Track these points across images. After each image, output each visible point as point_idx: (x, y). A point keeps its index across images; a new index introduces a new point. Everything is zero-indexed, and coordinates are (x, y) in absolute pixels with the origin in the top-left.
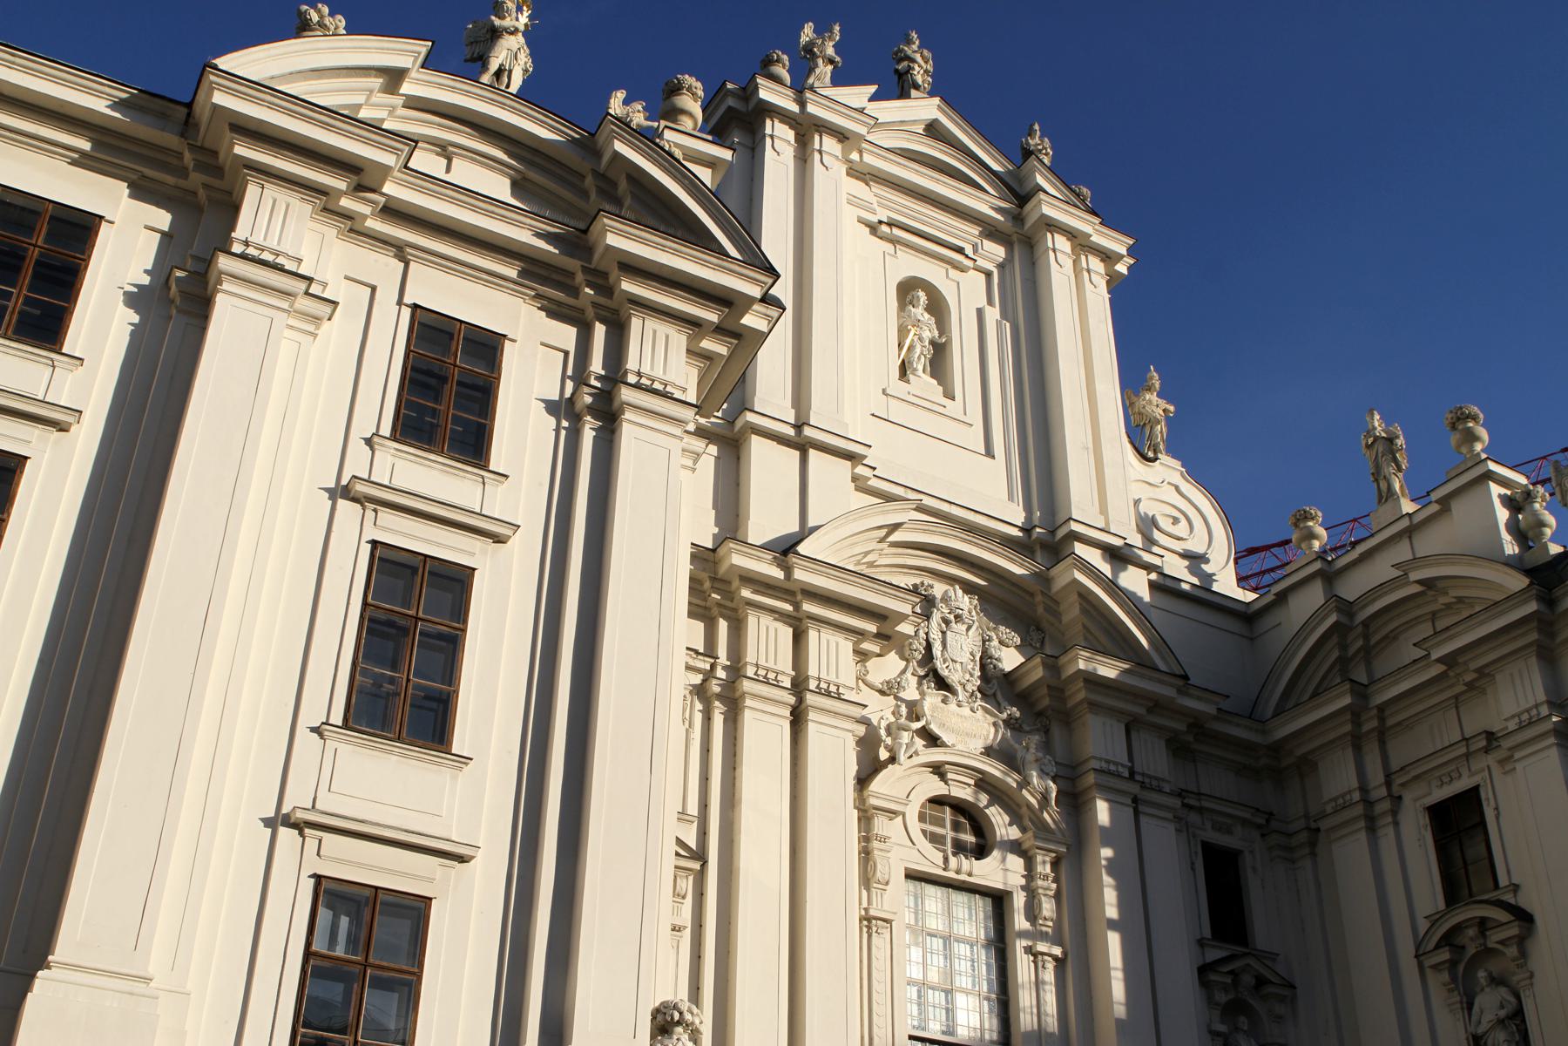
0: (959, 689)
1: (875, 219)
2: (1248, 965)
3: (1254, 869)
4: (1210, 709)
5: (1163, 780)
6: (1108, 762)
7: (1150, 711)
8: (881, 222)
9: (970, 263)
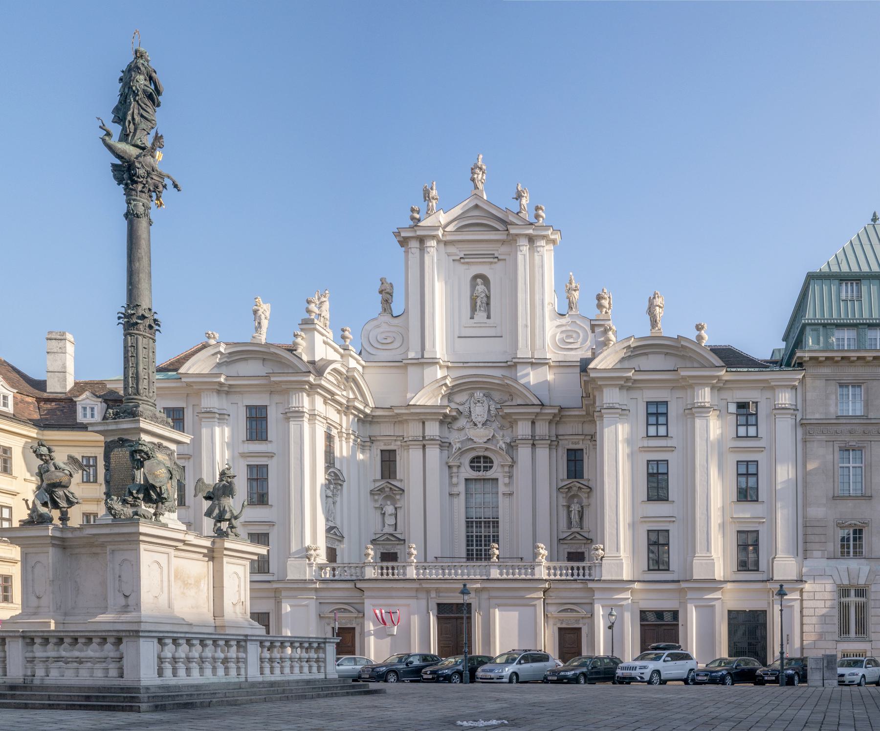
3: (586, 453)
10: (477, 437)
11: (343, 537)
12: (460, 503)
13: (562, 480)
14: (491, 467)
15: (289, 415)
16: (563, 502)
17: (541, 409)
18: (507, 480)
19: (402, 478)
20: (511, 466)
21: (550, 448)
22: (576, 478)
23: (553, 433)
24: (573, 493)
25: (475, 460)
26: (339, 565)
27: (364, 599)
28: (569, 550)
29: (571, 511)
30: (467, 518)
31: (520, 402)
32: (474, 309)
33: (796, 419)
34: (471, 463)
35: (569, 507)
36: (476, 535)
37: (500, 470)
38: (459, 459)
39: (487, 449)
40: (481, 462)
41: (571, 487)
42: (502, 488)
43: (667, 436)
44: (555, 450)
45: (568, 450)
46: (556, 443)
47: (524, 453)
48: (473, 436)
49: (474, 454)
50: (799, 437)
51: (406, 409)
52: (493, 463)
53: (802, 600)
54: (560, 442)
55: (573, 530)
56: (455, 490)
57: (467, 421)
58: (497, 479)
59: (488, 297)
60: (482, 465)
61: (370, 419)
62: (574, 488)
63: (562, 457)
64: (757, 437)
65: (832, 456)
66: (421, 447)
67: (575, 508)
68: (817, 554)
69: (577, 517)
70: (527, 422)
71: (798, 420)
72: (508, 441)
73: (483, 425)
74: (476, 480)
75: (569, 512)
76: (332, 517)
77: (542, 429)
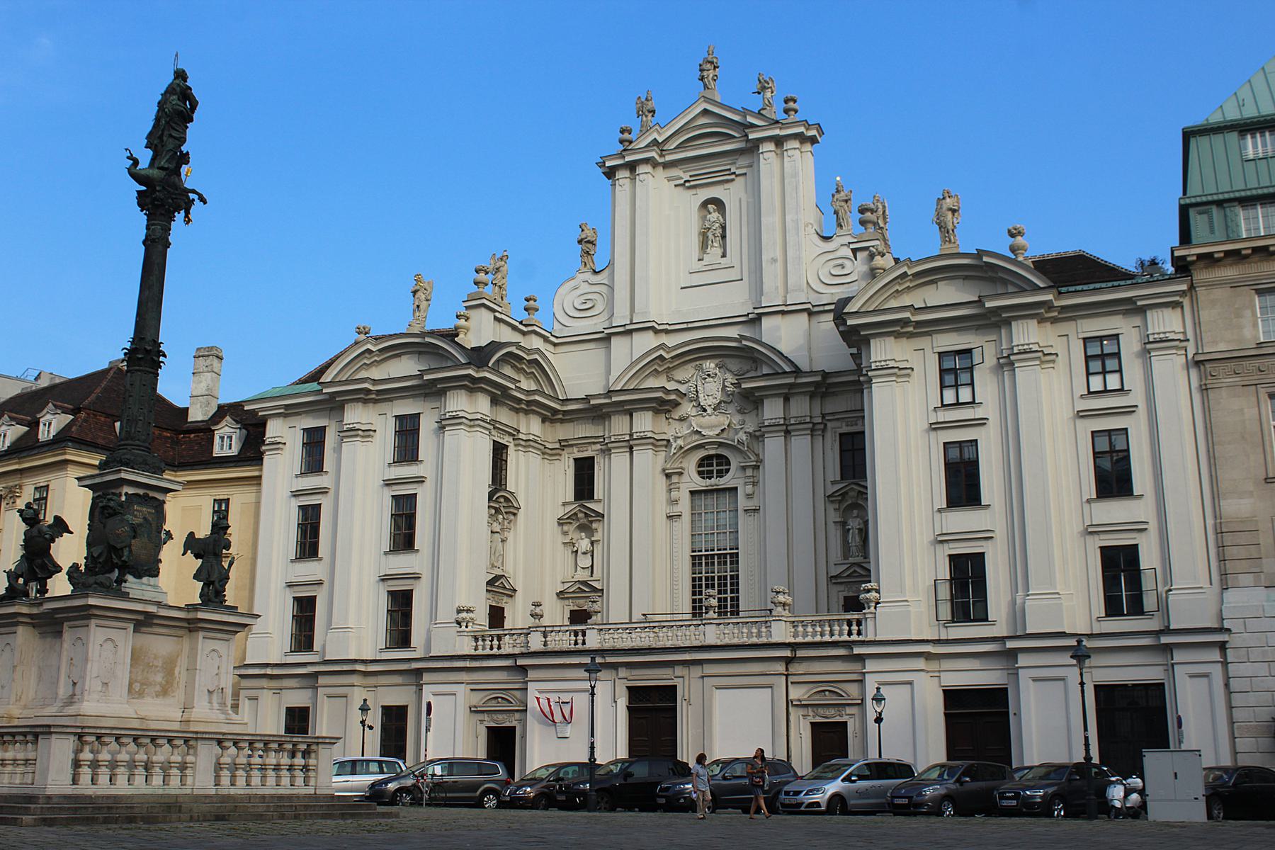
0: (707, 408)
1: (682, 182)
2: (852, 488)
4: (818, 378)
5: (805, 416)
6: (772, 419)
7: (789, 389)
8: (685, 181)
9: (733, 177)
10: (704, 428)
11: (515, 590)
12: (684, 527)
13: (833, 483)
14: (729, 469)
15: (444, 423)
16: (834, 516)
17: (796, 378)
18: (749, 489)
19: (601, 498)
20: (756, 467)
21: (812, 436)
22: (854, 478)
23: (817, 412)
24: (850, 502)
25: (702, 462)
26: (506, 632)
27: (526, 682)
28: (846, 594)
29: (849, 530)
30: (693, 552)
31: (766, 371)
32: (704, 245)
33: (1186, 355)
34: (699, 467)
35: (844, 524)
36: (731, 576)
37: (740, 474)
38: (681, 462)
39: (721, 445)
40: (713, 464)
41: (846, 493)
42: (742, 503)
43: (973, 402)
44: (821, 438)
45: (841, 435)
46: (822, 426)
47: (773, 446)
48: (701, 427)
49: (702, 453)
50: (1195, 383)
51: (605, 398)
52: (730, 465)
53: (1225, 664)
54: (829, 425)
55: (851, 560)
56: (676, 510)
57: (694, 406)
58: (736, 488)
59: (724, 228)
60: (715, 468)
61: (560, 416)
62: (851, 494)
63: (832, 446)
64: (1122, 389)
65: (1257, 409)
66: (628, 450)
67: (854, 524)
68: (1247, 579)
69: (858, 539)
70: (777, 399)
71: (1190, 356)
72: (751, 430)
73: (714, 409)
74: (706, 492)
75: (846, 532)
76: (501, 561)
77: (800, 407)
